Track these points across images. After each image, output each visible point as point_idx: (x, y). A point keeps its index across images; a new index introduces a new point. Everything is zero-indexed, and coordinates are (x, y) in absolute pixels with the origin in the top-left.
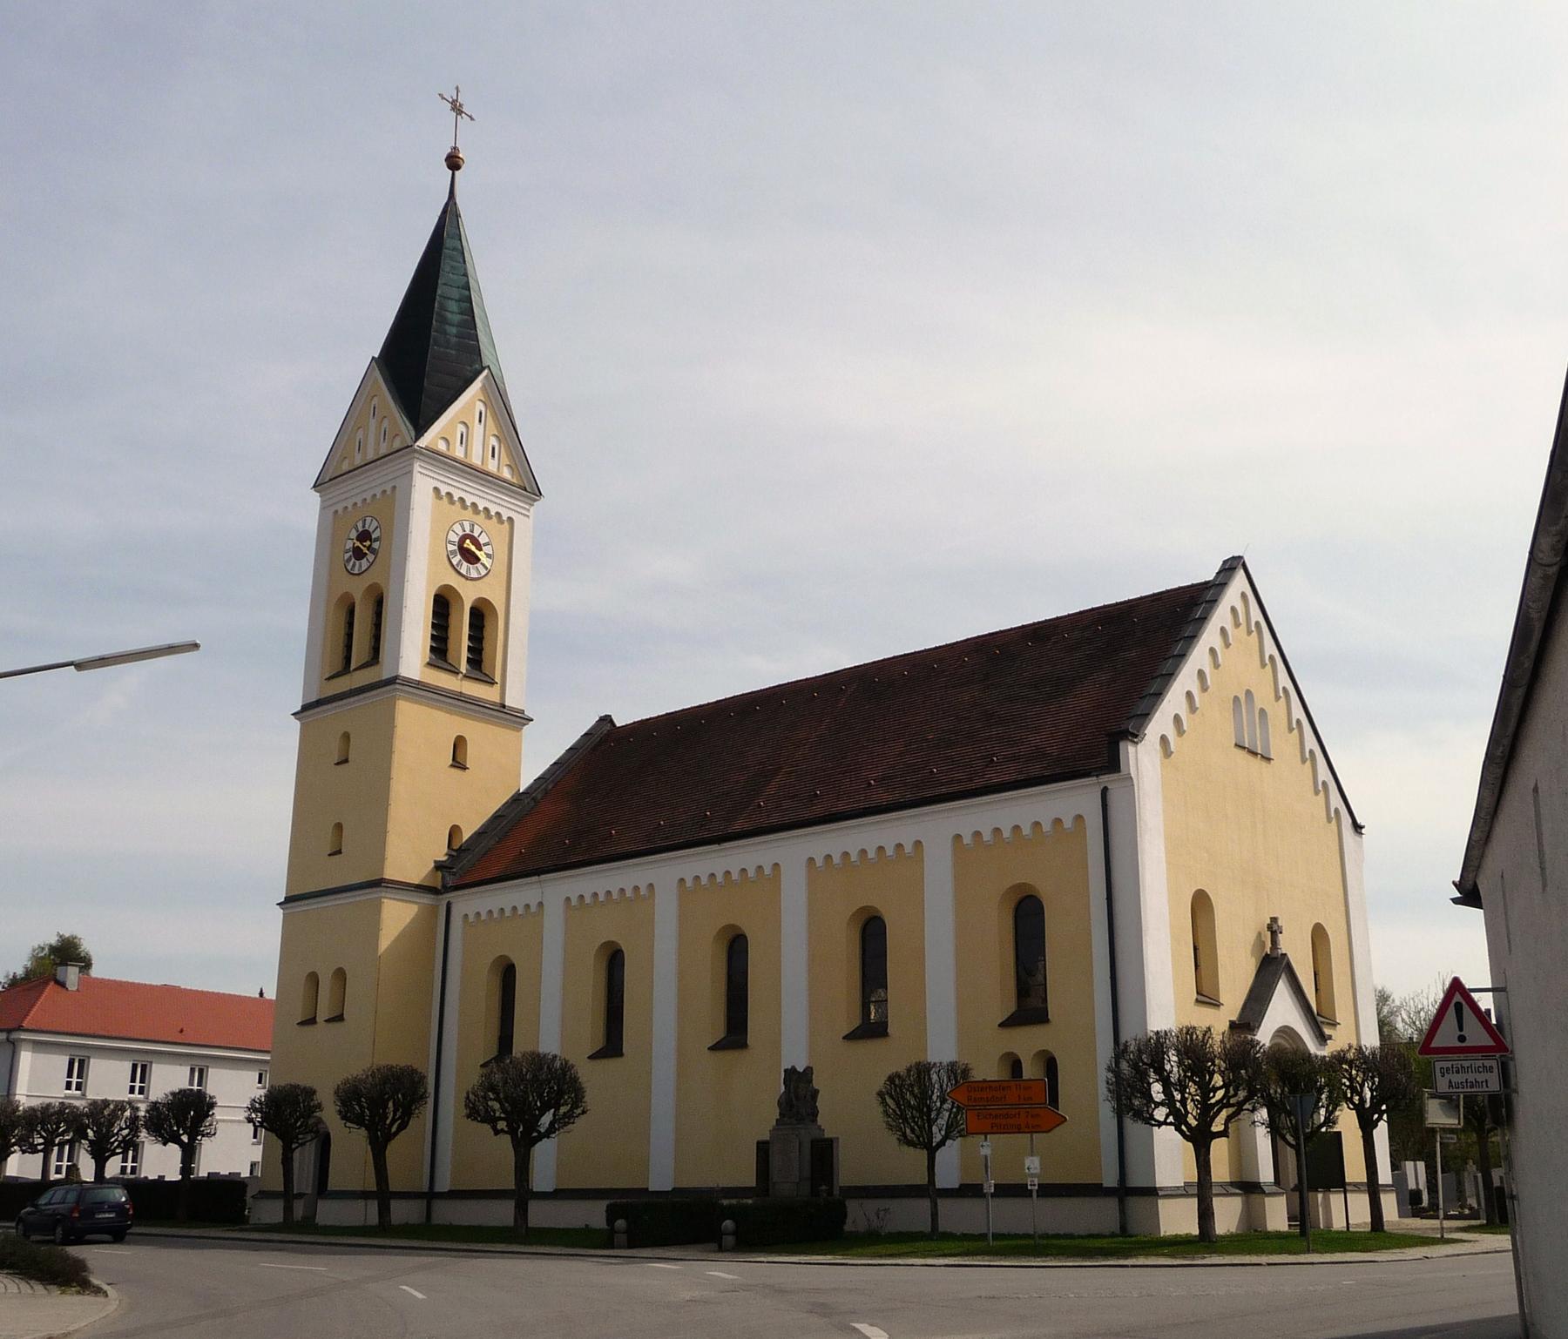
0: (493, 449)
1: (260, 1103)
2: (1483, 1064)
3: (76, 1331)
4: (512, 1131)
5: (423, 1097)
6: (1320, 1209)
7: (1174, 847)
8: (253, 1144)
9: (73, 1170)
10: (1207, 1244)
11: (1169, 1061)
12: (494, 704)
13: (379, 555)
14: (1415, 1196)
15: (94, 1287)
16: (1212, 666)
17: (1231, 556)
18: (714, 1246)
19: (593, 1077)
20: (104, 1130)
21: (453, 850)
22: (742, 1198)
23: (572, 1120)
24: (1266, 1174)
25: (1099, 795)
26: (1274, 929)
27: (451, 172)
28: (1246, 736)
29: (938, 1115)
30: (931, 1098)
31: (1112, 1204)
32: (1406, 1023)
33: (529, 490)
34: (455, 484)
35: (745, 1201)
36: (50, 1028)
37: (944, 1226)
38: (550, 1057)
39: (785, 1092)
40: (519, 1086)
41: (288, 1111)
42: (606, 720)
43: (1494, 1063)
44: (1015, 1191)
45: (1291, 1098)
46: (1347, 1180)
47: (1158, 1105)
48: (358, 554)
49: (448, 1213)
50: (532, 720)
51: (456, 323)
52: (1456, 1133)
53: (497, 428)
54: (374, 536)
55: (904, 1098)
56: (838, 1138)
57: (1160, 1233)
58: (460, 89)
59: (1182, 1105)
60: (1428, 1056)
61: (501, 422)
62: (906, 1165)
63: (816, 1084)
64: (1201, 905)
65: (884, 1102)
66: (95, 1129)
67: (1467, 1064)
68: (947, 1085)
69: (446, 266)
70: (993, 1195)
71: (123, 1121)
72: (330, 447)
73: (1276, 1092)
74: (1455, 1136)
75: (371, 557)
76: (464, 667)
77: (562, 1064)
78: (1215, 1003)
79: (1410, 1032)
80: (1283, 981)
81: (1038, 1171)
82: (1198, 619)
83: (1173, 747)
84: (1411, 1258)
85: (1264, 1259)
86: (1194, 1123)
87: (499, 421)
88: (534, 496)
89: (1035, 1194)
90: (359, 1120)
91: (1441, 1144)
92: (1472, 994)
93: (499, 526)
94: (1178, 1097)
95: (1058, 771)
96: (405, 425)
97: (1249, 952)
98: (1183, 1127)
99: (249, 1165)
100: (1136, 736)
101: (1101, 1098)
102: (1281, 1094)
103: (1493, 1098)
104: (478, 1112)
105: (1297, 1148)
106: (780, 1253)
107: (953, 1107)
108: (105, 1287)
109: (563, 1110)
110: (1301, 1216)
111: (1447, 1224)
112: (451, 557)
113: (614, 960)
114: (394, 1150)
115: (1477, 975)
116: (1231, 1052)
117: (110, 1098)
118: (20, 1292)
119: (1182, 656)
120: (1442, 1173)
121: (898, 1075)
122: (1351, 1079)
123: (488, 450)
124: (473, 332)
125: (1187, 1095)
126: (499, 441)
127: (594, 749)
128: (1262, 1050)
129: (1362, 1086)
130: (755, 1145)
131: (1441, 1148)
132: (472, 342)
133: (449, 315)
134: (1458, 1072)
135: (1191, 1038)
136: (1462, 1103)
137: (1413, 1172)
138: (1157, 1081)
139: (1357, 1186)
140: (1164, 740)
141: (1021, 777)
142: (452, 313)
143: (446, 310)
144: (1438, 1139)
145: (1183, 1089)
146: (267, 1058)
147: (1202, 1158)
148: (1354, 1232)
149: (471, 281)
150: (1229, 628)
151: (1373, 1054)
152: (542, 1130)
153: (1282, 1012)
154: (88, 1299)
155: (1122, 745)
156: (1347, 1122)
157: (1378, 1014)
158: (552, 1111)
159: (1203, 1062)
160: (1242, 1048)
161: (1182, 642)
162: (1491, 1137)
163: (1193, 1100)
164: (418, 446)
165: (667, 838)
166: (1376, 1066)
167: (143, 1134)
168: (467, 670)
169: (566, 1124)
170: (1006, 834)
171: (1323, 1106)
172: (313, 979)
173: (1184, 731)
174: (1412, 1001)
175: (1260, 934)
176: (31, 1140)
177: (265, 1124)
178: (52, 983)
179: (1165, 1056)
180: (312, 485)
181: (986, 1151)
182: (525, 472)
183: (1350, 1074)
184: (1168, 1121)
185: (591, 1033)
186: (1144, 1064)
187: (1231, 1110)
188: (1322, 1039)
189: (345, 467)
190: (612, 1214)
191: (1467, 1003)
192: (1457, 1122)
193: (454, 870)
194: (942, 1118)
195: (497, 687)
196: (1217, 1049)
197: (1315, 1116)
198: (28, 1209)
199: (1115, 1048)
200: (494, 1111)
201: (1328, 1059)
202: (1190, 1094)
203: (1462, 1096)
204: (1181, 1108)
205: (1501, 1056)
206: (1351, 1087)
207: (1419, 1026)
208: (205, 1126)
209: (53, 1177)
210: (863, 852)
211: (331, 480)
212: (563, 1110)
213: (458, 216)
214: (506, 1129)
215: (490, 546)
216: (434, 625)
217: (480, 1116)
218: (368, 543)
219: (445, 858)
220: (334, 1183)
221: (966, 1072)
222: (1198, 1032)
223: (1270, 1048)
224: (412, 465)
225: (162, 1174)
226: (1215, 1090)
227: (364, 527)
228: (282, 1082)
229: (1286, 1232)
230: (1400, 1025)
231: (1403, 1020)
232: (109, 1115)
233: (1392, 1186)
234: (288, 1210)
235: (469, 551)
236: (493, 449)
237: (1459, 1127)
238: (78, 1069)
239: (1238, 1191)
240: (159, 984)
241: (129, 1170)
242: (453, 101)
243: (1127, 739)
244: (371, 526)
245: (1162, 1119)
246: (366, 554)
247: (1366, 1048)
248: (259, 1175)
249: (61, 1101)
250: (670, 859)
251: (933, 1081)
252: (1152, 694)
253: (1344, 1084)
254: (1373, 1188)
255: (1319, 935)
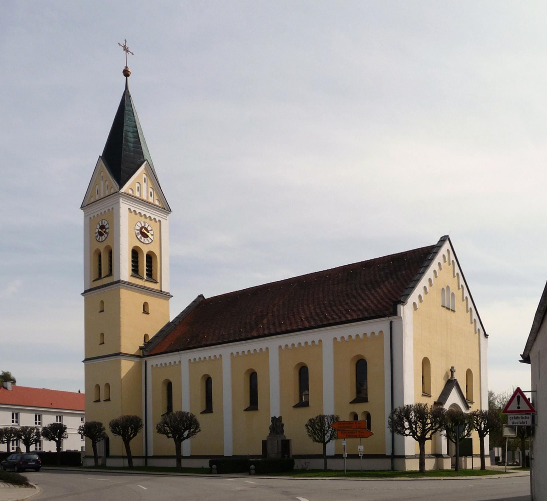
0: (151, 193)
1: (83, 428)
2: (526, 416)
3: (26, 499)
4: (174, 437)
5: (141, 426)
6: (463, 463)
7: (417, 343)
8: (82, 441)
9: (18, 449)
10: (422, 473)
11: (411, 415)
12: (158, 290)
13: (109, 234)
14: (497, 459)
15: (30, 485)
16: (434, 277)
17: (444, 235)
18: (248, 473)
19: (202, 419)
20: (28, 436)
21: (146, 342)
22: (257, 458)
23: (195, 434)
24: (444, 451)
25: (389, 323)
26: (452, 371)
27: (125, 77)
28: (446, 303)
29: (327, 432)
30: (325, 427)
31: (389, 461)
32: (499, 403)
33: (166, 209)
34: (137, 207)
35: (258, 459)
36: (3, 403)
37: (329, 467)
38: (186, 413)
39: (272, 425)
40: (176, 422)
41: (93, 430)
42: (201, 296)
43: (530, 416)
44: (356, 456)
45: (455, 427)
46: (473, 453)
47: (406, 429)
48: (101, 234)
49: (152, 463)
50: (173, 296)
51: (132, 142)
52: (514, 439)
53: (152, 184)
54: (106, 227)
55: (315, 427)
56: (291, 440)
57: (405, 469)
58: (127, 41)
59: (415, 429)
60: (506, 414)
61: (154, 182)
62: (317, 448)
63: (283, 422)
64: (426, 363)
65: (307, 428)
66: (24, 436)
67: (519, 416)
68: (331, 423)
69: (126, 118)
70: (346, 458)
71: (34, 433)
72: (86, 192)
73: (450, 425)
74: (513, 440)
75: (106, 235)
76: (145, 277)
77: (191, 415)
78: (429, 396)
79: (500, 405)
80: (455, 388)
81: (363, 450)
82: (430, 259)
83: (418, 307)
84: (494, 478)
85: (442, 478)
86: (419, 435)
87: (152, 182)
88: (168, 212)
89: (361, 458)
90: (119, 433)
91: (508, 442)
92: (524, 393)
93: (155, 223)
94: (414, 426)
95: (374, 315)
96: (115, 183)
97: (443, 378)
98: (416, 436)
99: (81, 447)
100: (404, 303)
101: (386, 427)
102: (451, 426)
103: (528, 427)
104: (161, 431)
105: (456, 443)
106: (271, 476)
107: (332, 430)
108: (35, 485)
109: (192, 430)
110: (456, 465)
111: (508, 467)
112: (137, 235)
113: (208, 381)
114: (132, 443)
115: (526, 386)
116: (434, 412)
117: (28, 426)
118: (5, 487)
119: (423, 273)
120: (508, 451)
121: (313, 419)
122: (477, 421)
123: (149, 194)
124: (139, 145)
125: (417, 426)
126: (153, 190)
127: (197, 307)
128: (445, 411)
129: (481, 423)
130: (261, 442)
131: (508, 443)
132: (139, 150)
133: (129, 139)
134: (516, 419)
135: (420, 407)
136: (517, 429)
137: (497, 452)
138: (407, 421)
139: (477, 456)
140: (414, 304)
141: (360, 317)
142: (130, 137)
143: (128, 137)
144: (507, 440)
145: (416, 424)
146: (84, 413)
147: (422, 446)
148: (474, 470)
149: (137, 124)
150: (442, 263)
151: (486, 413)
152: (185, 437)
153: (454, 398)
154: (29, 489)
155: (398, 306)
156: (475, 435)
157: (489, 399)
158: (188, 430)
159: (424, 415)
160: (438, 410)
161: (423, 268)
162: (526, 440)
163: (419, 428)
164: (121, 192)
165: (226, 338)
166: (486, 416)
167: (42, 438)
168: (146, 278)
169: (193, 435)
170: (354, 337)
171: (466, 430)
172: (98, 387)
173: (422, 301)
174: (501, 395)
175: (447, 372)
176: (2, 439)
177: (85, 434)
178: (2, 388)
179: (410, 413)
180: (80, 207)
181: (344, 444)
182: (165, 202)
183: (477, 419)
184: (410, 434)
185: (201, 405)
186: (402, 416)
187: (433, 431)
188: (468, 407)
189: (92, 200)
190: (211, 463)
191: (522, 396)
192: (514, 435)
193: (147, 350)
194: (329, 433)
195: (159, 284)
196: (429, 411)
197: (463, 433)
198: (4, 461)
199: (392, 411)
200: (167, 430)
201: (469, 414)
202: (418, 425)
203: (517, 427)
204: (415, 430)
205: (533, 413)
206: (478, 424)
207: (504, 403)
208: (64, 435)
209: (11, 451)
210: (300, 344)
211: (87, 205)
212: (192, 430)
213: (130, 97)
214: (172, 436)
215: (152, 231)
216: (132, 261)
217: (162, 432)
218: (104, 230)
219: (143, 345)
220: (111, 453)
221: (337, 418)
222: (422, 405)
223: (448, 411)
224: (119, 199)
225: (50, 450)
226: (428, 424)
227: (102, 223)
228: (90, 421)
229: (451, 470)
230: (496, 403)
231: (498, 401)
232: (29, 431)
233: (489, 455)
234: (96, 462)
235: (144, 233)
236: (151, 193)
237: (515, 436)
238: (15, 416)
239: (434, 457)
240: (41, 388)
241: (38, 449)
242: (124, 46)
243: (400, 303)
244: (105, 223)
245: (408, 434)
246: (104, 234)
247: (484, 411)
248: (85, 451)
249: (11, 427)
250: (227, 346)
251: (326, 421)
252: (411, 287)
253: (475, 423)
254: (482, 456)
255: (469, 373)
